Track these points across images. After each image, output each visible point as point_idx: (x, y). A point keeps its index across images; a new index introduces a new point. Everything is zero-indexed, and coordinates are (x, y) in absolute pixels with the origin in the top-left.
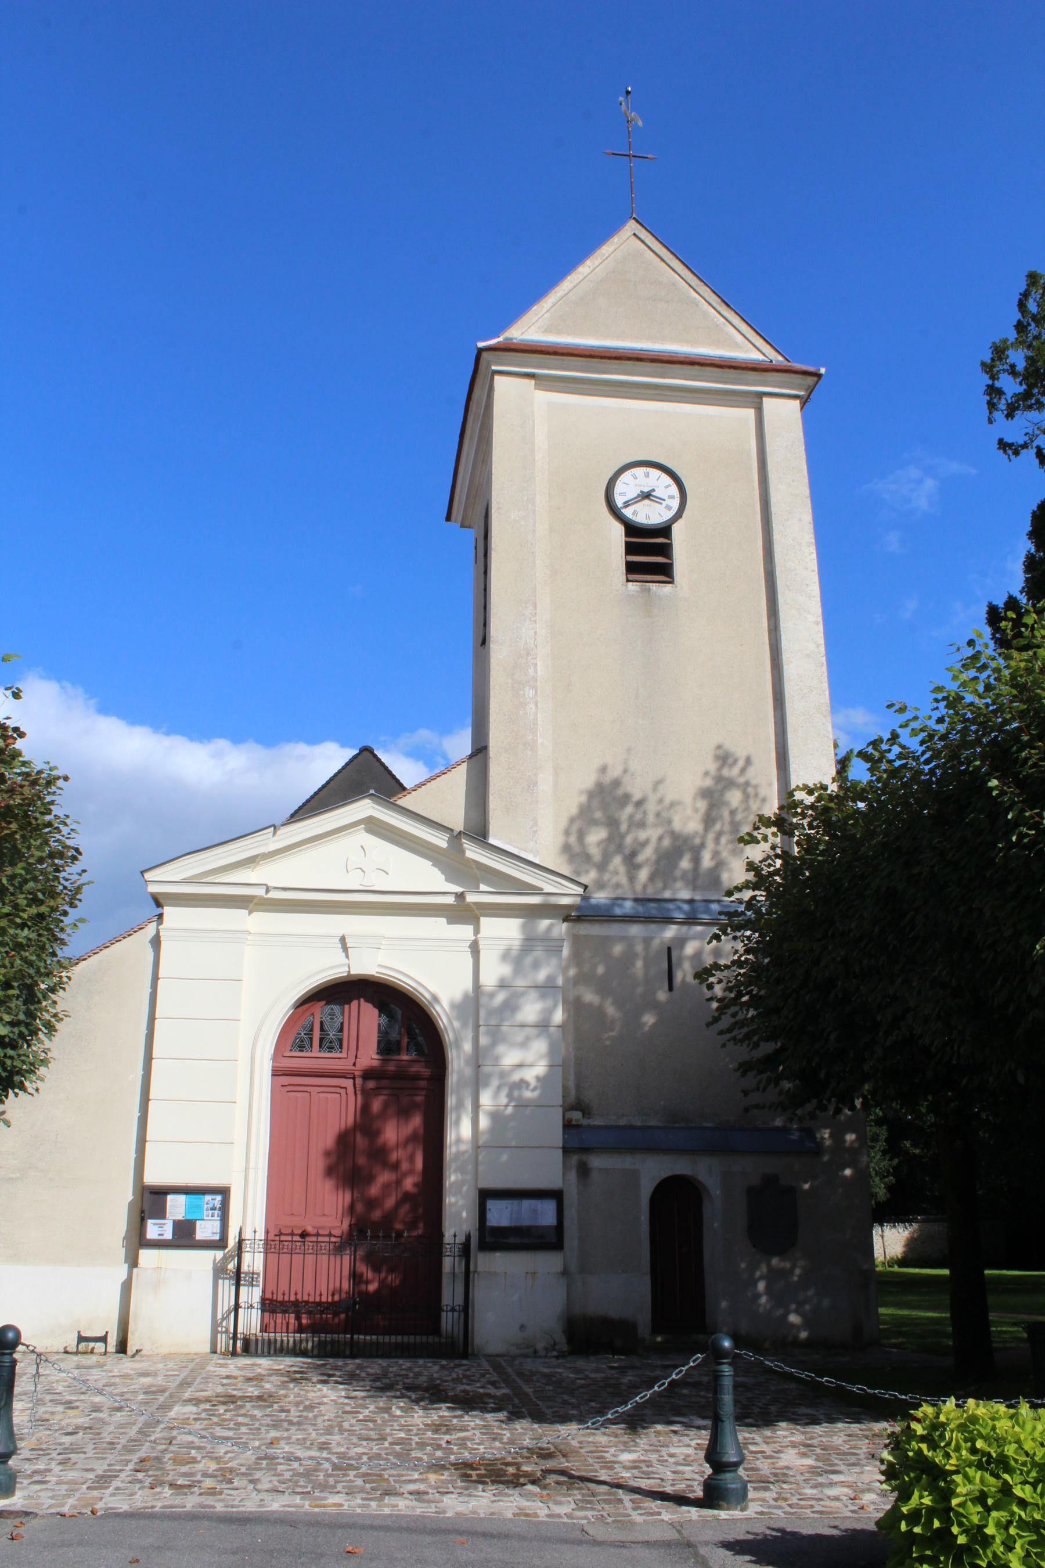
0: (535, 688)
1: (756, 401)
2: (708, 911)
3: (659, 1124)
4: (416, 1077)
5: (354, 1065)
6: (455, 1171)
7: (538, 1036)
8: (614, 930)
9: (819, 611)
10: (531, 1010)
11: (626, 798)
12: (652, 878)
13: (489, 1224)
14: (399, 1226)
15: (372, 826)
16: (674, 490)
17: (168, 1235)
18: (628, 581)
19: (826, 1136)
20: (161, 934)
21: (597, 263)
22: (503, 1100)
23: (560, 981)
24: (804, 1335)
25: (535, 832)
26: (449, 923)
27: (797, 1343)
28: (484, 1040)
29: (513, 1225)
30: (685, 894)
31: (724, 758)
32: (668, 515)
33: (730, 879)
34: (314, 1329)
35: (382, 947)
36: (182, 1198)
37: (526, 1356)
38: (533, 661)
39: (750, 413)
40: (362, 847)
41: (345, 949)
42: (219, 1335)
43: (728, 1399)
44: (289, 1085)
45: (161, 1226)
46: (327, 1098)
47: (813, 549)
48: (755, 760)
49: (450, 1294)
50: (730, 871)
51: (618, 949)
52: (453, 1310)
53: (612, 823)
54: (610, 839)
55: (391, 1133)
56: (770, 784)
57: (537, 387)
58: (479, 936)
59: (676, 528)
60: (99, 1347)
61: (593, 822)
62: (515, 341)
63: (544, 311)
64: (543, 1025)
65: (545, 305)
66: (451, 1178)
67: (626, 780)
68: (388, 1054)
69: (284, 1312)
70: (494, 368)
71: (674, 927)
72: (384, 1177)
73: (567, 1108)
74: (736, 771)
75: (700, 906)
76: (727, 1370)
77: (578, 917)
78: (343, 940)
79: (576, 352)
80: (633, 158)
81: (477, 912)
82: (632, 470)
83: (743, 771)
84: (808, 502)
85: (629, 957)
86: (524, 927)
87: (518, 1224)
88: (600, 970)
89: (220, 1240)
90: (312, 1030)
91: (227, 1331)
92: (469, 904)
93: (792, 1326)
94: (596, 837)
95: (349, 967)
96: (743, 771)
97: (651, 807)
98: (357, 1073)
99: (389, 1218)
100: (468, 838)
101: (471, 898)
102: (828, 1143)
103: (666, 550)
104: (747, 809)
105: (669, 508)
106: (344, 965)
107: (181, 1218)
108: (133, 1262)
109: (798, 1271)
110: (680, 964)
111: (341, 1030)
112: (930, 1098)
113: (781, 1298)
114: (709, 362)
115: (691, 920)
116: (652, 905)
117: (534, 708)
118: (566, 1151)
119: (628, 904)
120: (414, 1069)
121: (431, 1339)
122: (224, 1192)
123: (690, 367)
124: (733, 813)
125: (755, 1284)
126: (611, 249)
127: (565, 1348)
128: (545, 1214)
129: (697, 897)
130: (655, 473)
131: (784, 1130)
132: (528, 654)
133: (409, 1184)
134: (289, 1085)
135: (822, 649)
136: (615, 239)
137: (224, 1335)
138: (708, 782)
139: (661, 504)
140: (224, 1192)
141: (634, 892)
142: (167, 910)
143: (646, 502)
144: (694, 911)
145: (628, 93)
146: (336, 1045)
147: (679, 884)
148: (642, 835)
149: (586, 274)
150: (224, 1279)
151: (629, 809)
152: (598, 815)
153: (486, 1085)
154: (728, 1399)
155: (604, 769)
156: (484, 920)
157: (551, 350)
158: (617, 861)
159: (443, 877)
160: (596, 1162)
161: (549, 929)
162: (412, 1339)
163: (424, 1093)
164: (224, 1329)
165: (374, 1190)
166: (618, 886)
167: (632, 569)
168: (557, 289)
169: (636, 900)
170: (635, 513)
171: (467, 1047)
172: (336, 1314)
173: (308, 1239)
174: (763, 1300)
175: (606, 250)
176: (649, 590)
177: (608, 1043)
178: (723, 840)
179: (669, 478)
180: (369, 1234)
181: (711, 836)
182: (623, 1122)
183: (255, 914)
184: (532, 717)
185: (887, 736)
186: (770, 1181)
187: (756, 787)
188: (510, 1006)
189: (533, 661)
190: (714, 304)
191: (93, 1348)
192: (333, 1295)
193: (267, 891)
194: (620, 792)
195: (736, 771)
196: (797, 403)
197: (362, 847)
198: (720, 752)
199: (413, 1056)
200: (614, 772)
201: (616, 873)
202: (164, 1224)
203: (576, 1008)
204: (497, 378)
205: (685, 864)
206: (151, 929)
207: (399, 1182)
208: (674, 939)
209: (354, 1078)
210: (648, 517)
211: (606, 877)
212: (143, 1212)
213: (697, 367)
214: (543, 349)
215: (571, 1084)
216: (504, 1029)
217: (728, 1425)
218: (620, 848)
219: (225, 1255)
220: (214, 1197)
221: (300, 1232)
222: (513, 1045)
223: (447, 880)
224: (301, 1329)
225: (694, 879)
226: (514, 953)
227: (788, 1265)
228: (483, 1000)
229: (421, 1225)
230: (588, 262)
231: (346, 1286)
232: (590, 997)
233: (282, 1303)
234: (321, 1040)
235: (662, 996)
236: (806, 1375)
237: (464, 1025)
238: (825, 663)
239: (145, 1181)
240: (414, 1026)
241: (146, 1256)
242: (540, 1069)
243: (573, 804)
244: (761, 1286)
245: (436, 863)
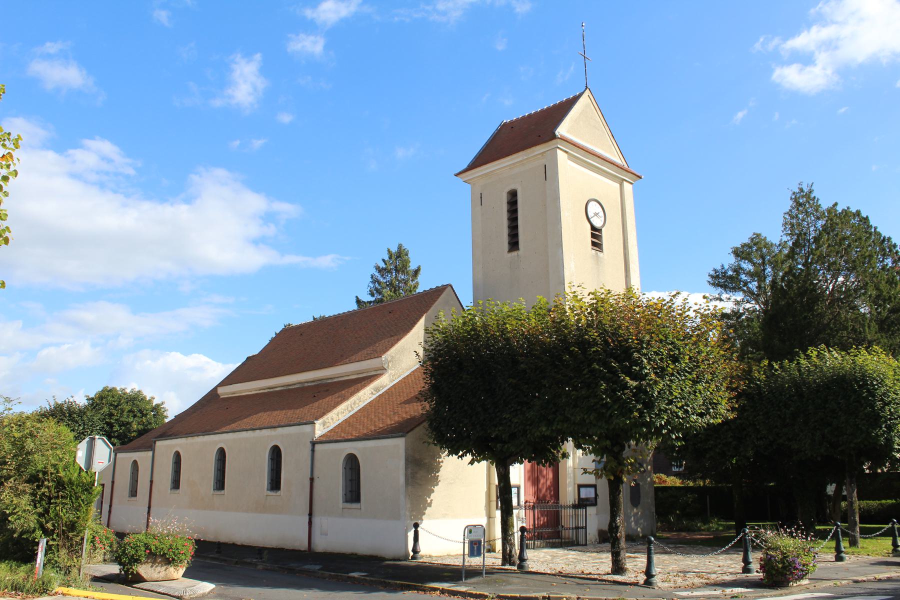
39: (618, 185)
57: (569, 159)
59: (603, 230)
70: (559, 146)
84: (635, 228)
93: (639, 532)
154: (840, 536)
157: (578, 146)
174: (633, 523)
176: (597, 254)
244: (632, 519)
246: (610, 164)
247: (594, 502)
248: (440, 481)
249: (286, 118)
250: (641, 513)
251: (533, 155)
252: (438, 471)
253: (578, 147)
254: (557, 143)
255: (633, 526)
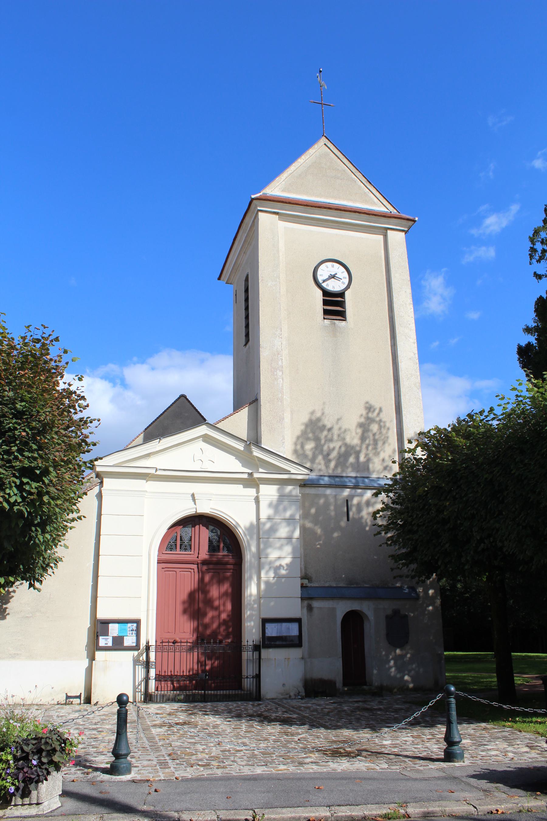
0: (282, 371)
1: (384, 232)
2: (363, 482)
3: (344, 585)
4: (227, 563)
5: (198, 557)
6: (249, 610)
7: (287, 544)
8: (321, 490)
9: (415, 337)
10: (283, 531)
11: (324, 426)
12: (336, 467)
13: (267, 635)
14: (220, 637)
15: (206, 438)
16: (346, 274)
17: (110, 644)
18: (324, 319)
19: (421, 590)
20: (103, 492)
21: (307, 157)
22: (272, 574)
23: (297, 517)
24: (411, 686)
25: (283, 442)
26: (244, 488)
27: (408, 689)
28: (262, 546)
29: (278, 635)
30: (353, 474)
31: (369, 408)
32: (343, 287)
33: (373, 467)
34: (180, 689)
35: (212, 499)
36: (116, 625)
37: (286, 699)
38: (281, 358)
39: (381, 237)
40: (201, 449)
41: (194, 500)
42: (137, 693)
43: (454, 713)
44: (166, 568)
45: (106, 639)
46: (184, 574)
47: (412, 306)
48: (383, 409)
49: (248, 670)
50: (374, 463)
51: (322, 501)
52: (253, 677)
53: (317, 439)
54: (316, 448)
55: (215, 592)
56: (391, 421)
57: (280, 219)
58: (259, 494)
59: (347, 293)
60: (77, 701)
61: (308, 439)
62: (268, 195)
63: (282, 180)
64: (289, 538)
65: (282, 178)
66: (247, 613)
67: (323, 418)
68: (214, 552)
69: (166, 681)
70: (259, 208)
71: (348, 490)
72: (211, 614)
73: (302, 578)
74: (375, 414)
75: (359, 479)
76: (453, 700)
77: (305, 484)
78: (193, 495)
79: (300, 203)
80: (323, 105)
81: (258, 482)
82: (326, 263)
83: (378, 414)
85: (327, 505)
86: (279, 490)
87: (281, 635)
88: (313, 511)
89: (136, 646)
90: (176, 540)
91: (141, 691)
92: (254, 478)
93: (407, 681)
94: (309, 446)
95: (196, 509)
96: (378, 414)
97: (336, 432)
98: (199, 562)
99: (215, 634)
100: (255, 445)
101: (256, 475)
102: (421, 594)
103: (342, 304)
104: (380, 433)
105: (343, 283)
106: (193, 508)
107: (116, 635)
108: (92, 658)
109: (409, 656)
110: (351, 509)
111: (191, 540)
112: (487, 574)
113: (401, 669)
114: (364, 212)
115: (356, 487)
116: (337, 479)
117: (282, 381)
118: (302, 599)
119: (326, 479)
120: (226, 559)
121: (240, 692)
122: (138, 622)
123: (354, 214)
124: (374, 435)
125: (389, 662)
126: (314, 151)
127: (304, 694)
128: (293, 630)
129: (358, 475)
130: (336, 265)
131: (401, 588)
132: (278, 354)
133: (224, 616)
134: (166, 568)
135: (417, 356)
136: (316, 146)
137: (139, 693)
138: (362, 420)
139: (340, 281)
140: (138, 622)
141: (329, 473)
142: (105, 480)
143: (333, 280)
144: (357, 482)
145: (320, 71)
146: (188, 547)
147: (350, 469)
148: (332, 445)
149: (302, 163)
150: (138, 665)
151: (325, 433)
152: (310, 435)
153: (263, 568)
154: (454, 713)
155: (313, 413)
156: (262, 487)
158: (320, 458)
159: (241, 464)
160: (316, 604)
161: (291, 491)
162: (231, 692)
163: (231, 571)
164: (139, 690)
165: (207, 620)
166: (320, 470)
167: (326, 312)
168: (288, 170)
169: (330, 476)
170: (327, 285)
171: (254, 549)
172: (191, 681)
173: (176, 644)
174: (393, 670)
175: (311, 151)
177: (318, 546)
178: (370, 448)
179: (343, 268)
180: (212, 641)
181: (364, 446)
182: (327, 585)
183: (149, 482)
184: (281, 386)
185: (487, 409)
186: (396, 612)
187: (384, 422)
188: (273, 529)
189: (281, 358)
190: (364, 182)
191: (72, 702)
192: (189, 672)
193: (156, 470)
194: (320, 424)
195: (375, 414)
196: (404, 233)
197: (201, 449)
198: (367, 405)
199: (225, 553)
200: (318, 414)
201: (320, 464)
202: (108, 639)
203: (303, 530)
204: (260, 213)
205: (352, 460)
206: (96, 490)
207: (219, 616)
208: (349, 496)
209: (198, 564)
210: (333, 287)
211: (315, 466)
212: (97, 633)
213: (357, 214)
214: (284, 201)
215: (303, 567)
216: (271, 540)
217: (454, 725)
218: (321, 452)
219: (139, 653)
220: (132, 624)
221: (172, 641)
222: (275, 548)
223: (242, 466)
224: (174, 689)
225: (357, 466)
226: (275, 502)
227: (404, 652)
228: (261, 526)
229: (231, 636)
230: (303, 157)
231: (196, 667)
232: (309, 525)
233: (164, 676)
234: (181, 545)
235: (343, 523)
236: (486, 702)
237: (251, 537)
238: (418, 362)
239: (97, 617)
240: (226, 538)
241: (99, 655)
242: (288, 560)
243: (299, 429)
244: (392, 663)
245: (237, 458)
246: (374, 216)
247: (297, 642)
248: (8, 614)
249: (474, 316)
250: (411, 655)
251: (248, 229)
252: (7, 602)
253: (290, 203)
254: (256, 206)
255: (392, 674)
